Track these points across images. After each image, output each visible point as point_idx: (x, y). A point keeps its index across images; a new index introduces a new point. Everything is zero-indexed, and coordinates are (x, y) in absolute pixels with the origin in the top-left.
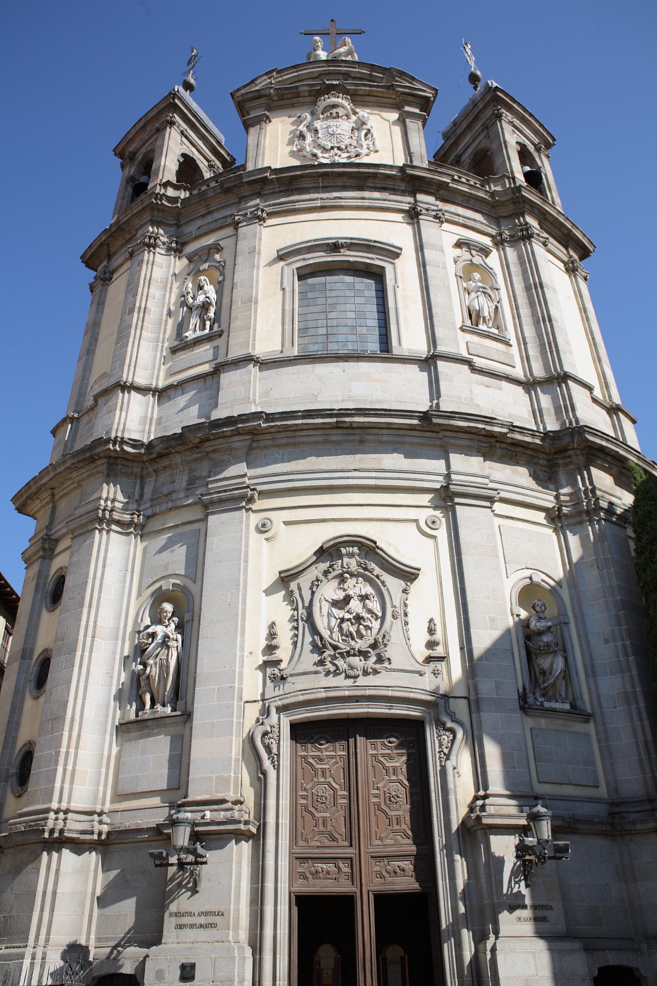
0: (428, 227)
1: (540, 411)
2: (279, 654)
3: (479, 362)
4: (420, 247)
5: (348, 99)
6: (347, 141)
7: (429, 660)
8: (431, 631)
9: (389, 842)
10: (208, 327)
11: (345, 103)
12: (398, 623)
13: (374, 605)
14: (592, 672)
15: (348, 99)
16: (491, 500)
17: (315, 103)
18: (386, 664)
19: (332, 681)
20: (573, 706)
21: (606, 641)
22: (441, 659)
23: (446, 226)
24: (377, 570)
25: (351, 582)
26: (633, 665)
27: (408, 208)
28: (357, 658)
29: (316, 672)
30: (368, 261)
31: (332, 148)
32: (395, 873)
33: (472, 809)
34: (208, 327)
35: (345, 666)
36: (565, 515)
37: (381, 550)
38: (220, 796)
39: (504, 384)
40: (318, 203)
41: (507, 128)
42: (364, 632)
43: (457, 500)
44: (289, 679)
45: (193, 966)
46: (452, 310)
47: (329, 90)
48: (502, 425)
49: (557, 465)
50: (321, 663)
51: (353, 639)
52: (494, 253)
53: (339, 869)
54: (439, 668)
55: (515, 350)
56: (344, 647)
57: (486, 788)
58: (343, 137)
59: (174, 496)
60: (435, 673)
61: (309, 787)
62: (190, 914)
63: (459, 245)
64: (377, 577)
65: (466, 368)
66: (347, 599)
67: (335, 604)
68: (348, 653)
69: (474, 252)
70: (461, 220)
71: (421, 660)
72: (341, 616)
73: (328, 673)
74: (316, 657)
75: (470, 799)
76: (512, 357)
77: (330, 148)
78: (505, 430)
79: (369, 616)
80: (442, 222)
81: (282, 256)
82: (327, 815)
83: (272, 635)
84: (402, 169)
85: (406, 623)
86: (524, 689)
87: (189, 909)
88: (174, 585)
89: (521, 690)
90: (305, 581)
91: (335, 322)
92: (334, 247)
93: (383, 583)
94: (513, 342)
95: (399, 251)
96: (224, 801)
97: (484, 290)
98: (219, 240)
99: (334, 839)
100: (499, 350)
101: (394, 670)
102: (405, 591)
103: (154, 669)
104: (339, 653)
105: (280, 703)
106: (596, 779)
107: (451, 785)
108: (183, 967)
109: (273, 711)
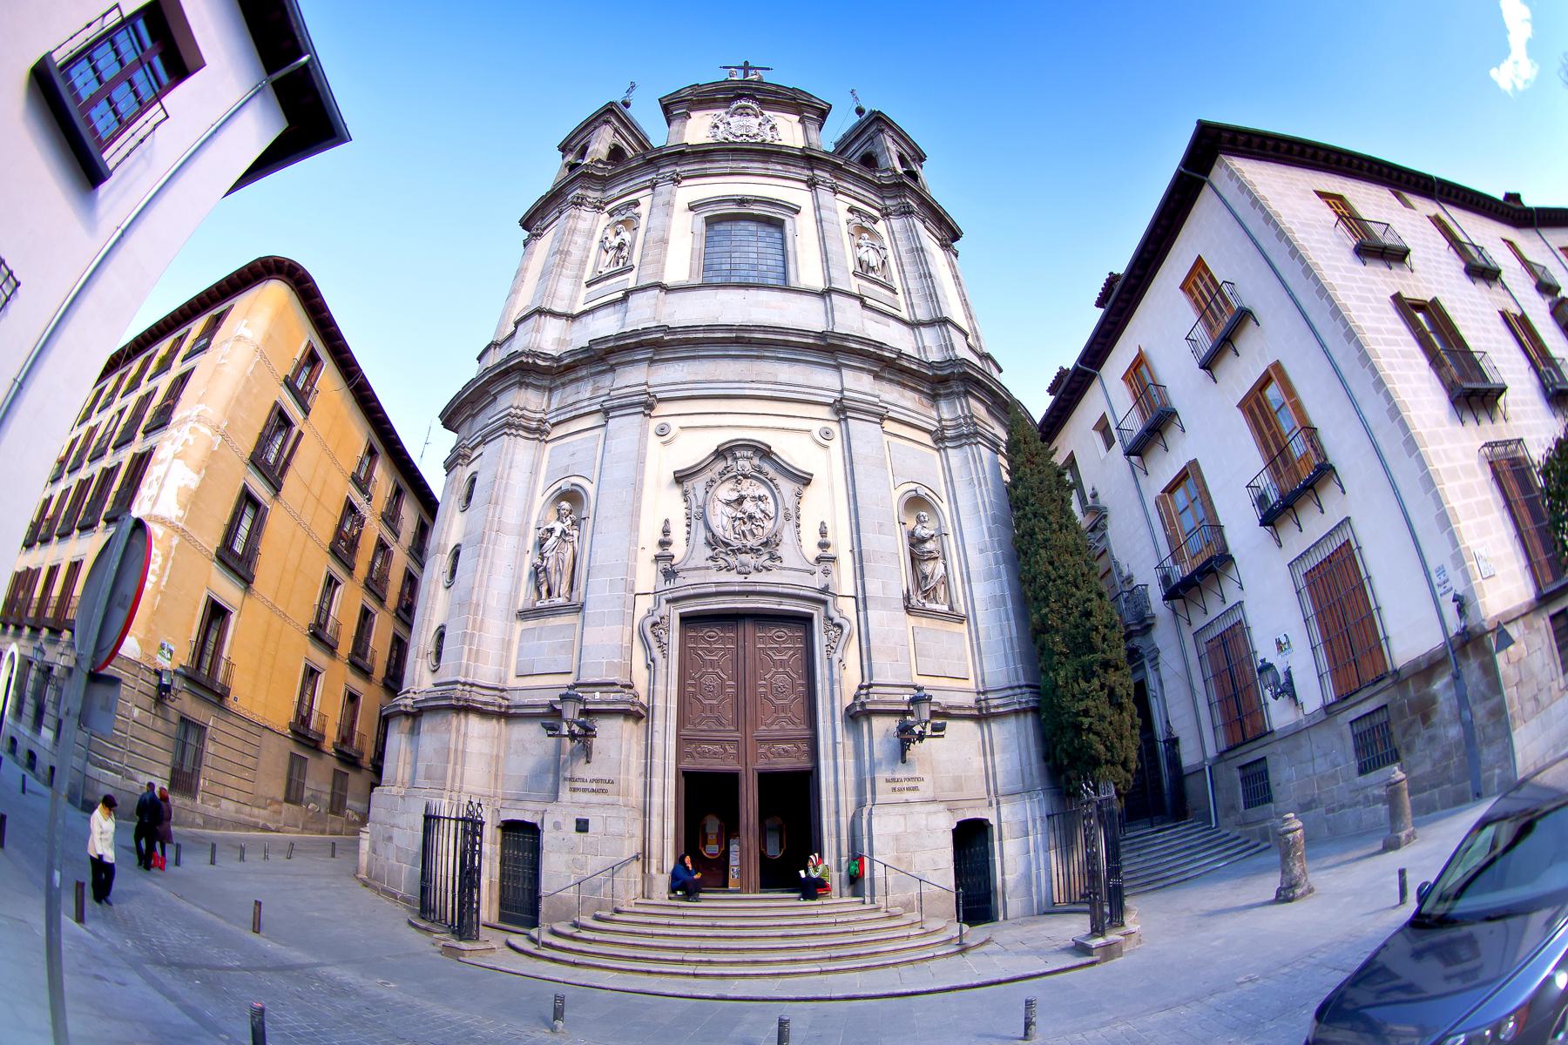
0: (825, 196)
1: (924, 347)
2: (672, 550)
3: (869, 301)
4: (818, 208)
6: (756, 131)
7: (819, 560)
8: (823, 533)
9: (774, 727)
10: (621, 264)
12: (790, 526)
13: (771, 508)
14: (967, 579)
16: (882, 418)
18: (778, 563)
19: (724, 576)
20: (951, 608)
21: (981, 551)
22: (833, 559)
23: (839, 196)
24: (772, 473)
25: (746, 483)
26: (1004, 573)
28: (749, 556)
29: (708, 568)
31: (742, 135)
32: (779, 754)
33: (856, 697)
34: (621, 264)
35: (737, 563)
36: (947, 438)
37: (775, 454)
38: (611, 679)
39: (892, 322)
40: (728, 171)
41: (889, 143)
42: (755, 531)
43: (849, 414)
44: (680, 574)
45: (586, 822)
46: (845, 257)
48: (891, 351)
49: (940, 395)
50: (713, 558)
51: (745, 536)
53: (725, 750)
54: (829, 568)
55: (900, 297)
56: (736, 544)
57: (871, 678)
59: (578, 406)
60: (826, 573)
61: (697, 676)
62: (583, 780)
63: (851, 210)
64: (771, 480)
65: (857, 303)
66: (740, 500)
67: (728, 503)
68: (739, 549)
69: (864, 219)
70: (852, 194)
71: (812, 560)
72: (734, 515)
73: (720, 569)
74: (709, 552)
75: (854, 690)
76: (898, 302)
78: (894, 356)
79: (761, 515)
80: (836, 193)
82: (715, 702)
83: (666, 532)
84: (802, 150)
85: (798, 526)
86: (908, 591)
87: (582, 776)
88: (572, 485)
89: (905, 592)
90: (699, 484)
91: (738, 261)
92: (742, 201)
93: (776, 486)
94: (899, 290)
96: (614, 684)
99: (721, 724)
101: (784, 569)
102: (799, 495)
103: (550, 562)
104: (731, 550)
105: (670, 596)
106: (967, 673)
107: (836, 676)
108: (578, 821)
109: (663, 602)
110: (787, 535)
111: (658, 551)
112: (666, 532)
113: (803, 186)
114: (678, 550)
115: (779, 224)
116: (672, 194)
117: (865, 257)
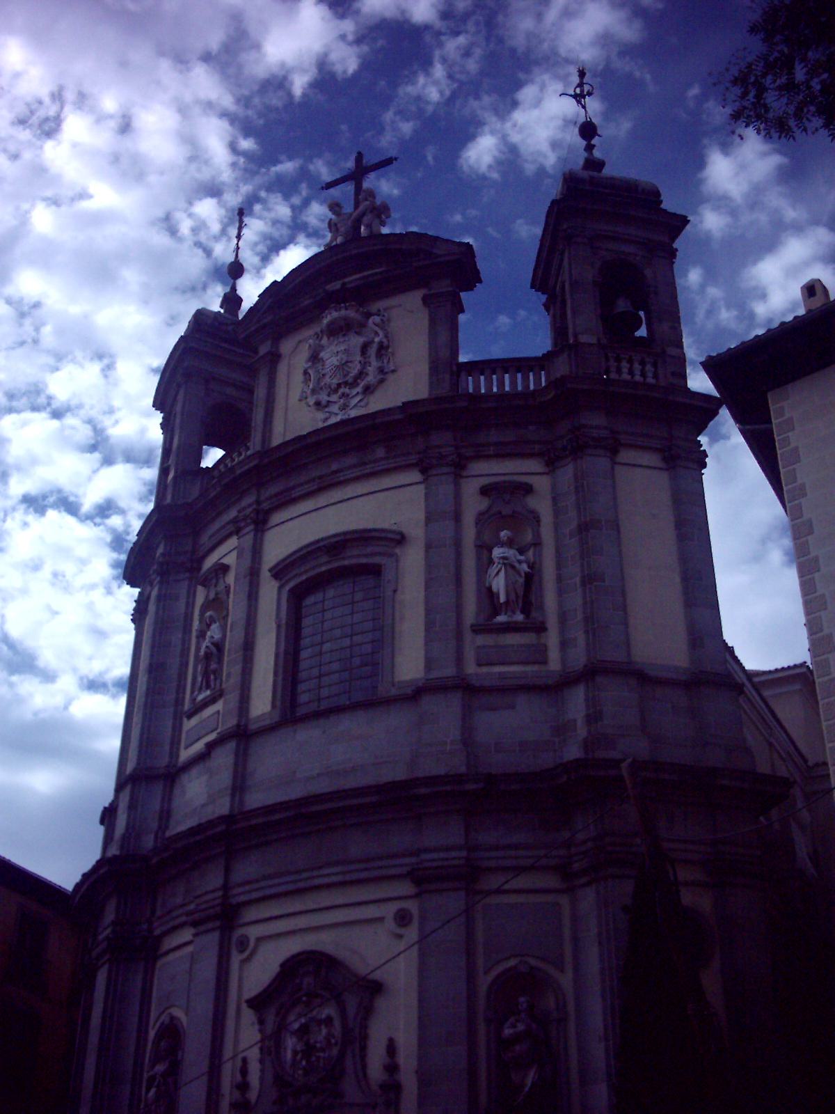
5: (353, 306)
7: (384, 1087)
11: (351, 314)
15: (353, 306)
17: (319, 318)
27: (414, 461)
30: (364, 561)
31: (339, 385)
39: (522, 700)
47: (322, 306)
52: (542, 484)
58: (350, 364)
59: (175, 914)
77: (336, 386)
81: (279, 572)
85: (363, 1048)
95: (398, 537)
97: (506, 561)
98: (220, 559)
100: (522, 646)
102: (367, 1011)
110: (349, 1063)
111: (237, 1094)
112: (244, 1071)
113: (415, 476)
114: (253, 1095)
115: (375, 571)
116: (257, 552)
117: (495, 589)
